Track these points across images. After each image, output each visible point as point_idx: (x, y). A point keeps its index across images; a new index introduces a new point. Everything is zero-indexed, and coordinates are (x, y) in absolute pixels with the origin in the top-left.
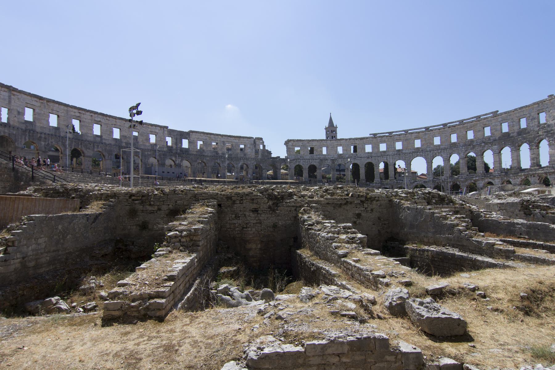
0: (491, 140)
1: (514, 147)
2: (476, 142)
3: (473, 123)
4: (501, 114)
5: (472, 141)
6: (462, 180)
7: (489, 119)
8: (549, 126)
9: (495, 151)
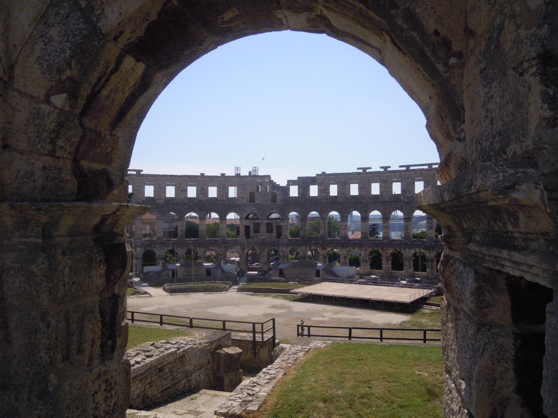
1: (161, 215)
7: (132, 177)
8: (199, 201)
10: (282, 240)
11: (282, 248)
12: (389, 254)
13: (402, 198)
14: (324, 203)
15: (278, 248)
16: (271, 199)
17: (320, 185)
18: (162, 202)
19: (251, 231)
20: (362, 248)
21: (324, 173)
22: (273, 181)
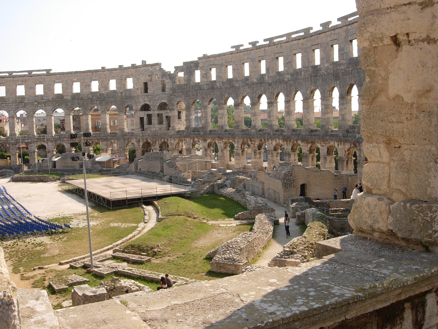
0: (44, 100)
2: (27, 99)
3: (24, 78)
4: (55, 74)
5: (22, 97)
6: (13, 142)
7: (43, 76)
8: (100, 95)
9: (49, 112)
10: (171, 132)
11: (170, 140)
12: (256, 146)
13: (266, 78)
14: (206, 89)
15: (168, 140)
16: (161, 88)
17: (202, 69)
18: (69, 98)
19: (145, 123)
20: (235, 139)
21: (205, 57)
22: (162, 69)
